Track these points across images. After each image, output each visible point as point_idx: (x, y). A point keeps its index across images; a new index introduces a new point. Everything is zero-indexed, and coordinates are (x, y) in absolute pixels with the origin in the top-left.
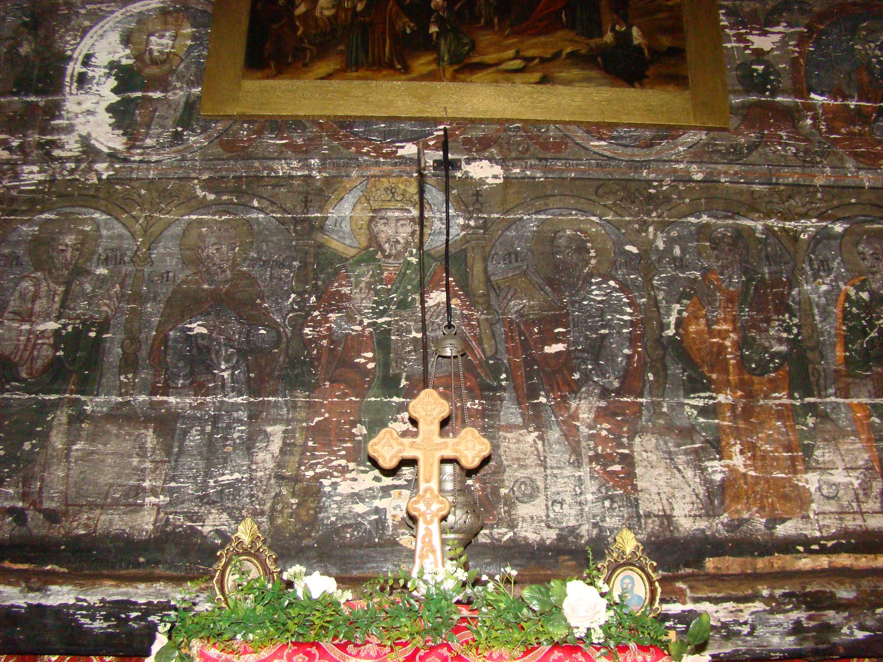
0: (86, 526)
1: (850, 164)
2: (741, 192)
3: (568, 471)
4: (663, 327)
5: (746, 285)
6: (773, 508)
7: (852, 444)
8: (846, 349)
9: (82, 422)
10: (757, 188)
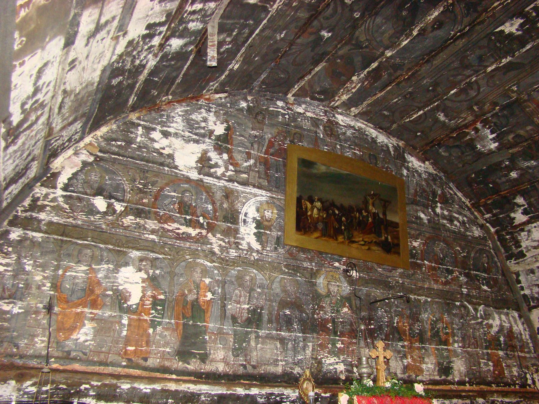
0: (264, 370)
1: (432, 282)
2: (410, 287)
4: (394, 323)
5: (410, 313)
10: (413, 286)
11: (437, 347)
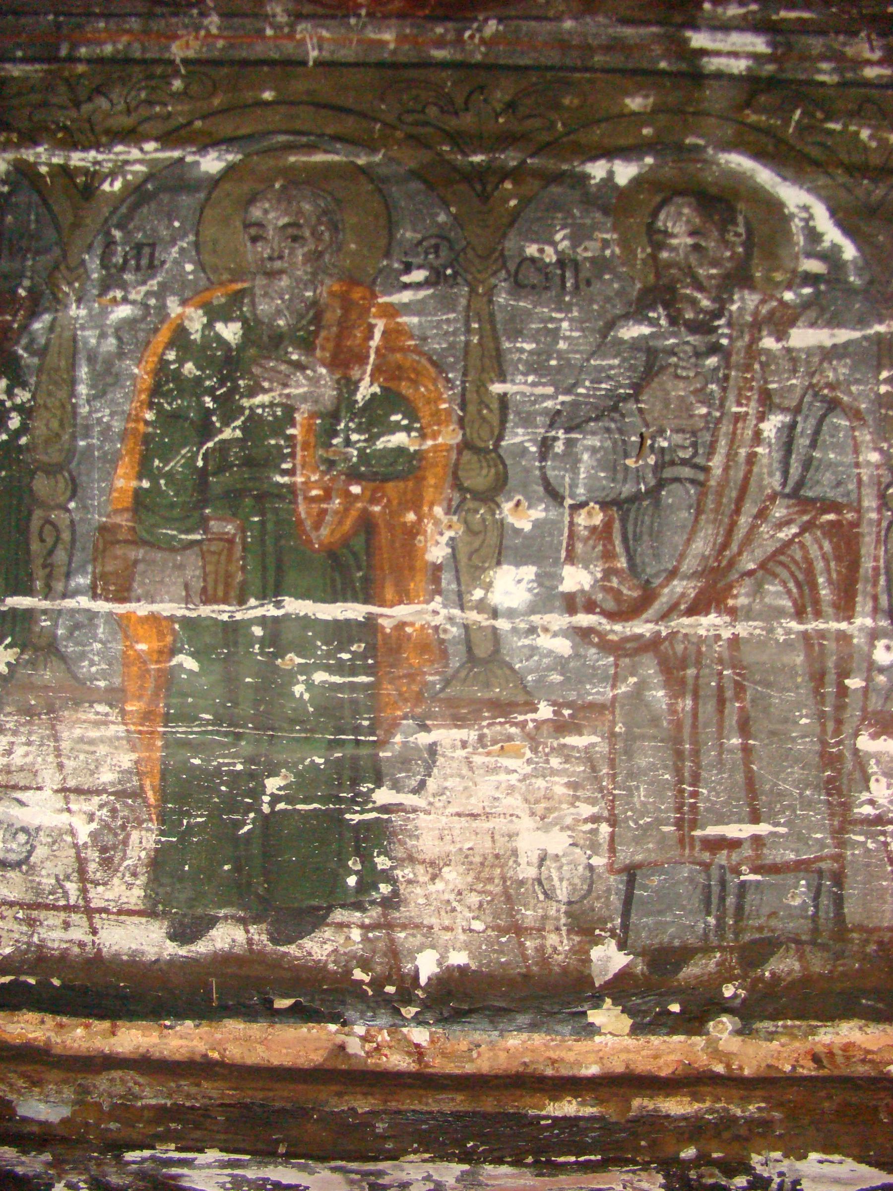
7: (97, 724)
8: (144, 469)
11: (222, 612)
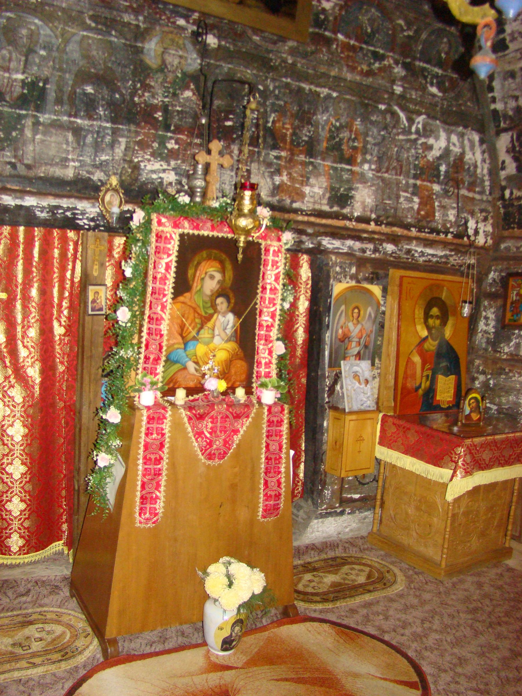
0: (44, 173)
1: (345, 69)
3: (228, 172)
4: (267, 122)
5: (298, 111)
6: (293, 198)
8: (327, 143)
9: (39, 125)
11: (335, 165)
